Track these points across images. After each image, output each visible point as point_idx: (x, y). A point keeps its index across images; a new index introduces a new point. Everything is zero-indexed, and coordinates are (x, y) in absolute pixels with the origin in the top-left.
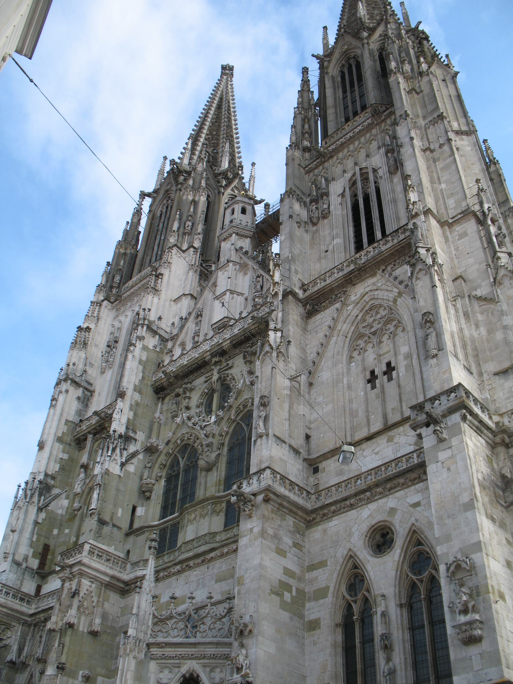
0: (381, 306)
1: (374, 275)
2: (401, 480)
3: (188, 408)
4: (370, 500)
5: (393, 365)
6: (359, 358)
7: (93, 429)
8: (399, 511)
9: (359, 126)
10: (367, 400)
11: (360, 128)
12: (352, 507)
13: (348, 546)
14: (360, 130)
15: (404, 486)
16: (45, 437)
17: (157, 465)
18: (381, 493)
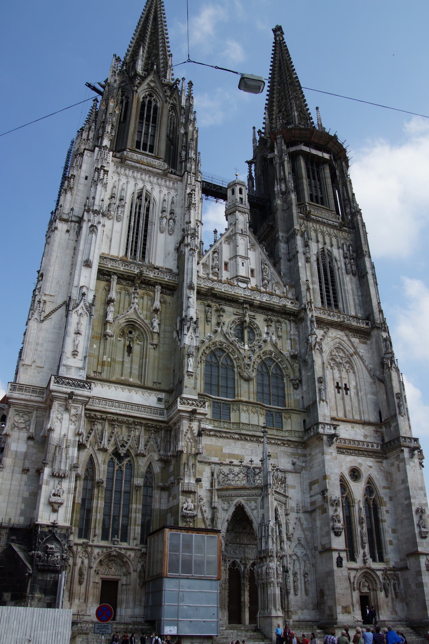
0: (342, 350)
1: (342, 330)
2: (366, 453)
3: (224, 324)
4: (351, 454)
5: (348, 387)
6: (331, 371)
7: (121, 274)
8: (363, 466)
9: (332, 221)
10: (335, 397)
11: (331, 222)
12: (343, 453)
13: (341, 471)
14: (330, 224)
15: (365, 456)
16: (91, 258)
17: (201, 351)
18: (356, 454)
